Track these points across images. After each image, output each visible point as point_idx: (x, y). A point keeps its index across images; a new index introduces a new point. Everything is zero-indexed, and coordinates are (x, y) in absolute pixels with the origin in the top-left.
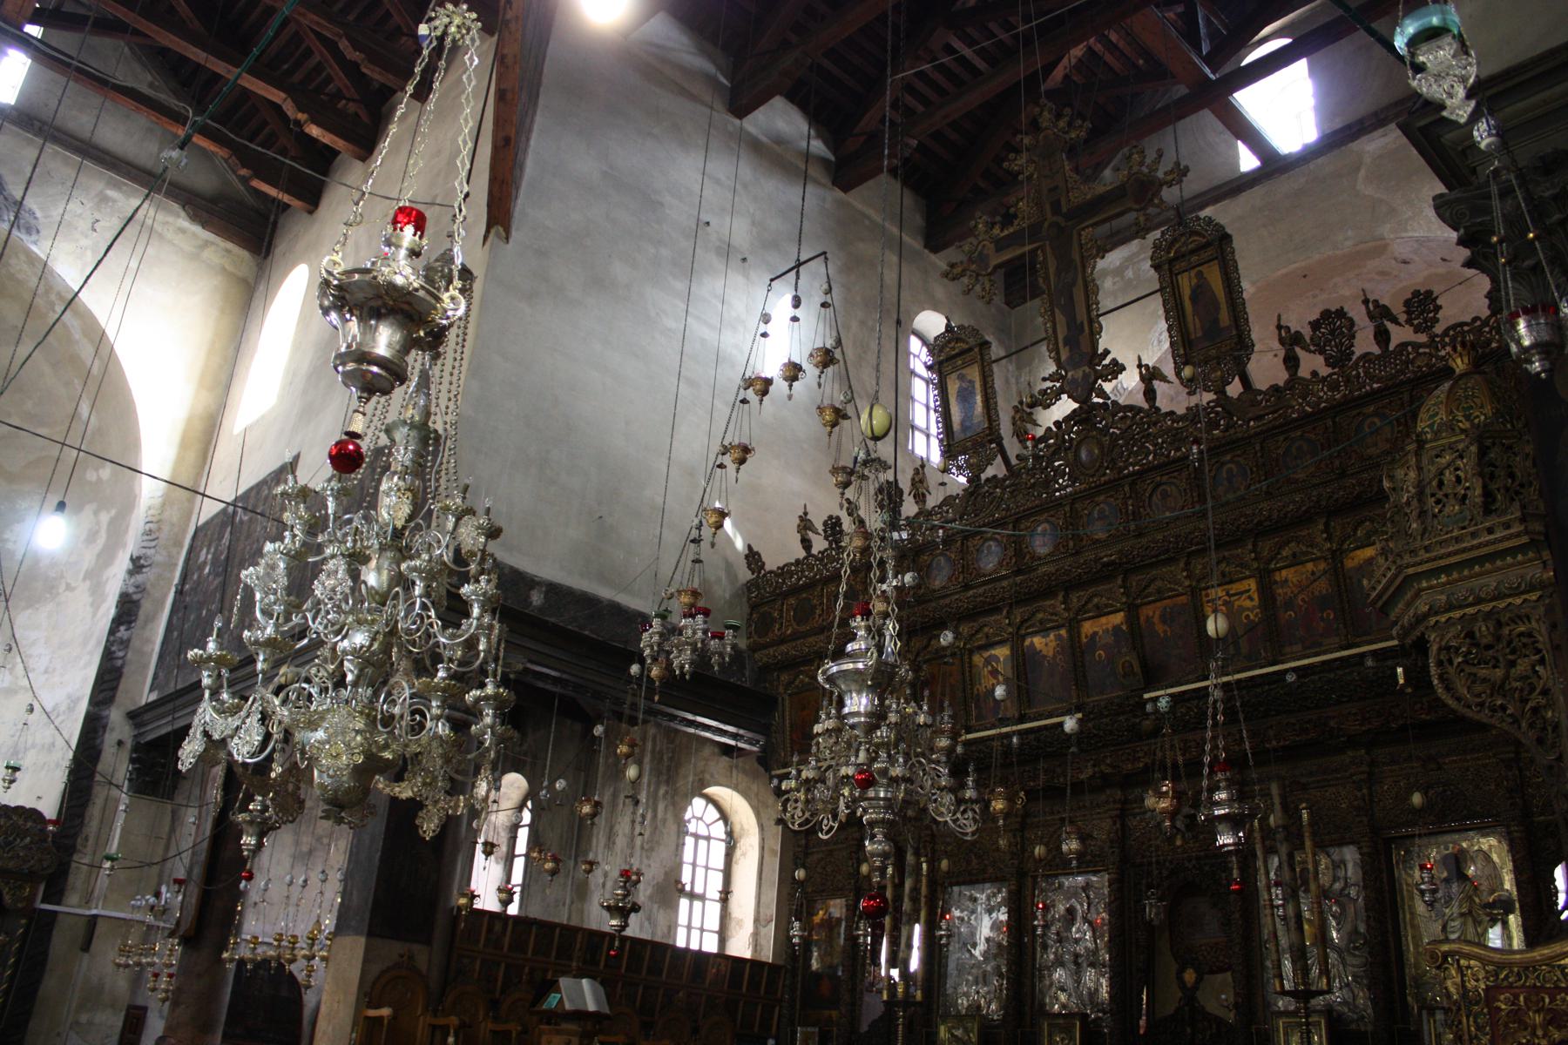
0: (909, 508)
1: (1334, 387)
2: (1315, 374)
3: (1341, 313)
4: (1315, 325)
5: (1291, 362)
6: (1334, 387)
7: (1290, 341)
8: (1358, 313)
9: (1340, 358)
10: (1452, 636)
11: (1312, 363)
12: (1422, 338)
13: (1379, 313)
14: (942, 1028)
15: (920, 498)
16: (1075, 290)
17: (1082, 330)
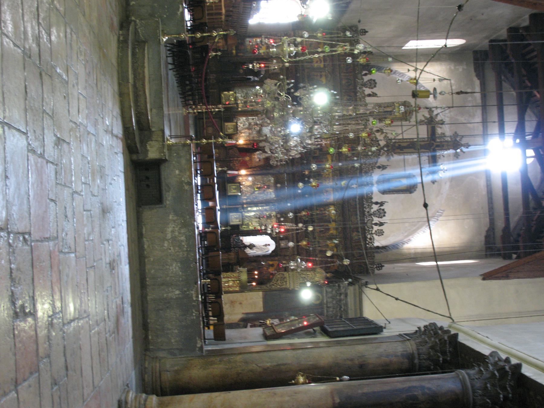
0: (368, 91)
1: (368, 212)
2: (372, 208)
3: (384, 216)
4: (383, 210)
5: (376, 203)
6: (368, 212)
7: (382, 204)
8: (382, 220)
9: (374, 214)
10: (285, 276)
11: (375, 208)
12: (373, 232)
13: (381, 224)
14: (232, 92)
15: (369, 95)
16: (413, 149)
17: (401, 150)
